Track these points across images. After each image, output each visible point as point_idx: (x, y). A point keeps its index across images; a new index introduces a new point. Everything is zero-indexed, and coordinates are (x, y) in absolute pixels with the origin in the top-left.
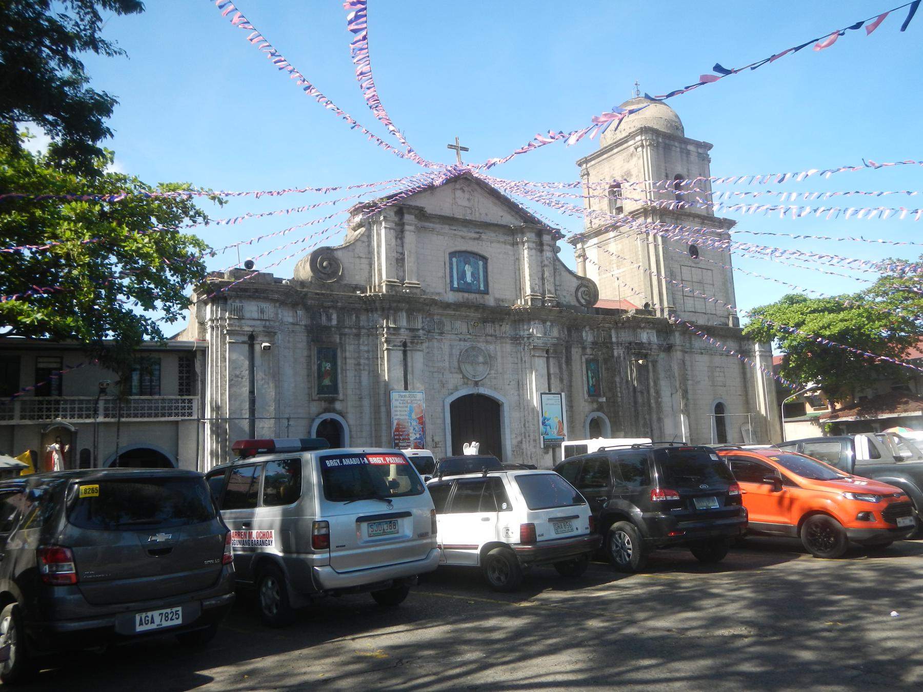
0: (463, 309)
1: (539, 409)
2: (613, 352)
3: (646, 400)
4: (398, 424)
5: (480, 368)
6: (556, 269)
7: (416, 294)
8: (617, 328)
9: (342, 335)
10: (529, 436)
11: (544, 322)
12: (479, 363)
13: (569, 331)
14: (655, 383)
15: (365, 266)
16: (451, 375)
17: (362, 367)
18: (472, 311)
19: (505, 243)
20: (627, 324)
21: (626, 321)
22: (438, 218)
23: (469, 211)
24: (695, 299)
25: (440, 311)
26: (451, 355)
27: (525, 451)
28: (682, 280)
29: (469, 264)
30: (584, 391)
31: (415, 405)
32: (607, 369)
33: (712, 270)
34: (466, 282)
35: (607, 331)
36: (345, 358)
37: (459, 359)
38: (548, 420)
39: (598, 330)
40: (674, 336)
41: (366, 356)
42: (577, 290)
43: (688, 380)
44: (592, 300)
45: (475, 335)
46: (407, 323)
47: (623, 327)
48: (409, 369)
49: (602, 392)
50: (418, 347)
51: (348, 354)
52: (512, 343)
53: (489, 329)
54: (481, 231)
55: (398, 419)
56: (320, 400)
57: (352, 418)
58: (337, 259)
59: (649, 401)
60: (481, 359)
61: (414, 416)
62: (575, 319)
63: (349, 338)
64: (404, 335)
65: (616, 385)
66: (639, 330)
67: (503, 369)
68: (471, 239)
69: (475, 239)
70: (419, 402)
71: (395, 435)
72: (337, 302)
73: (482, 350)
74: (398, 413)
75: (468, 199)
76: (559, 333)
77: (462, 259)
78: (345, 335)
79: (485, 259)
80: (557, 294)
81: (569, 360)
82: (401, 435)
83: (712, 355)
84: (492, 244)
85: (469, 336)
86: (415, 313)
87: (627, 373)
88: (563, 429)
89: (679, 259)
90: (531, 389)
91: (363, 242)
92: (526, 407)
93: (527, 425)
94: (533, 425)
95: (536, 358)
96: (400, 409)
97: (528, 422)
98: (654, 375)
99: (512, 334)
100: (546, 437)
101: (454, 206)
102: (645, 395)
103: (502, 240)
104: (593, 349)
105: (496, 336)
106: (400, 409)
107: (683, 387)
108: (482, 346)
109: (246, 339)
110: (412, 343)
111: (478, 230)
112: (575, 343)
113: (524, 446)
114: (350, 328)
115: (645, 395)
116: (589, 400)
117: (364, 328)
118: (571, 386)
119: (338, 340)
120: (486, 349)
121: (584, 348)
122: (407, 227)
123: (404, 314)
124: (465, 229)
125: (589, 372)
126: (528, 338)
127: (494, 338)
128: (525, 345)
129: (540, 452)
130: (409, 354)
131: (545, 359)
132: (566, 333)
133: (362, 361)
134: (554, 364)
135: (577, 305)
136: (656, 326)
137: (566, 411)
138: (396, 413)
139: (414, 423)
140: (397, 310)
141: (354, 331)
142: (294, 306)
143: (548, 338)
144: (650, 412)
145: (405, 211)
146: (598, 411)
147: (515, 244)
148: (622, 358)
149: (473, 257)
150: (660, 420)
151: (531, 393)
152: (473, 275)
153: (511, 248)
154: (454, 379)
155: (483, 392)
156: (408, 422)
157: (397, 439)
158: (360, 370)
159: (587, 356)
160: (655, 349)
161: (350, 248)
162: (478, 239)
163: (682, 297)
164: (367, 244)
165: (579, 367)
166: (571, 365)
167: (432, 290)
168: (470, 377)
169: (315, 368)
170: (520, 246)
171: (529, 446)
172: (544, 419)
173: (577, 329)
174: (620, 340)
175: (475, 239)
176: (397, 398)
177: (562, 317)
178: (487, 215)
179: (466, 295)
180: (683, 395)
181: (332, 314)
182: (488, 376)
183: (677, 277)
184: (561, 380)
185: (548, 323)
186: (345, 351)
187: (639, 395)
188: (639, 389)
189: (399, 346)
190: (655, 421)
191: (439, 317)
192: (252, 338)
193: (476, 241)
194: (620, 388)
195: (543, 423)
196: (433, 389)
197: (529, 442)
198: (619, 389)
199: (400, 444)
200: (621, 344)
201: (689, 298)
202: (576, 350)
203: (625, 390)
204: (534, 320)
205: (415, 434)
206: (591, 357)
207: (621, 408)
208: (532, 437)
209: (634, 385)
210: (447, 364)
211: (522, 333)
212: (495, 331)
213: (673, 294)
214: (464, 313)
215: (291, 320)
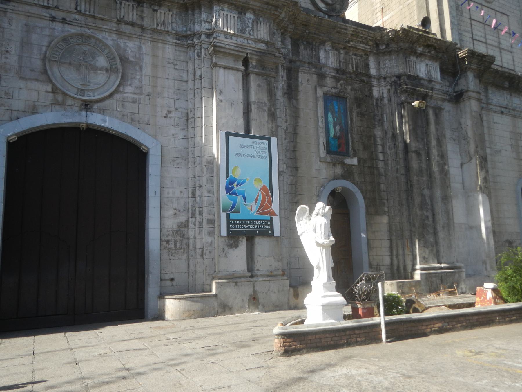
1: (222, 161)
2: (371, 90)
3: (424, 166)
5: (100, 78)
8: (378, 54)
10: (201, 213)
12: (95, 69)
13: (295, 44)
16: (22, 84)
20: (393, 46)
21: (392, 40)
24: (488, 46)
27: (191, 241)
28: (471, 19)
30: (318, 145)
32: (361, 115)
33: (508, 16)
35: (361, 56)
37: (46, 52)
39: (346, 53)
40: (466, 77)
44: (338, 6)
45: (94, 17)
47: (388, 52)
49: (351, 149)
52: (177, 45)
60: (102, 61)
62: (306, 25)
66: (413, 58)
67: (154, 87)
73: (106, 46)
76: (272, 35)
85: (77, 16)
87: (393, 122)
88: (270, 203)
90: (209, 126)
92: (198, 160)
93: (198, 193)
94: (209, 192)
95: (221, 71)
97: (201, 186)
98: (437, 130)
99: (180, 30)
100: (233, 215)
102: (424, 157)
104: (337, 79)
105: (142, 27)
107: (481, 152)
112: (306, 65)
113: (191, 233)
115: (424, 157)
116: (329, 159)
118: (295, 133)
120: (118, 47)
125: (330, 115)
126: (209, 35)
127: (138, 31)
128: (201, 49)
129: (219, 243)
131: (240, 75)
132: (290, 47)
134: (259, 86)
135: (311, 7)
136: (440, 55)
137: (280, 173)
143: (248, 39)
144: (430, 187)
146: (345, 179)
148: (386, 101)
150: (446, 198)
151: (209, 134)
155: (101, 124)
159: (326, 89)
160: (438, 90)
163: (471, 40)
165: (311, 105)
166: (297, 100)
168: (72, 93)
171: (200, 231)
172: (232, 182)
173: (308, 43)
174: (383, 73)
180: (481, 164)
182: (117, 96)
183: (464, 14)
184: (272, 116)
185: (250, 16)
187: (413, 156)
188: (413, 146)
190: (440, 199)
194: (383, 146)
195: (229, 189)
197: (201, 224)
198: (380, 148)
200: (385, 78)
201: (480, 43)
202: (307, 76)
203: (390, 149)
206: (334, 91)
207: (383, 178)
208: (205, 215)
209: (405, 142)
211: (197, 28)
212: (142, 18)
213: (460, 34)
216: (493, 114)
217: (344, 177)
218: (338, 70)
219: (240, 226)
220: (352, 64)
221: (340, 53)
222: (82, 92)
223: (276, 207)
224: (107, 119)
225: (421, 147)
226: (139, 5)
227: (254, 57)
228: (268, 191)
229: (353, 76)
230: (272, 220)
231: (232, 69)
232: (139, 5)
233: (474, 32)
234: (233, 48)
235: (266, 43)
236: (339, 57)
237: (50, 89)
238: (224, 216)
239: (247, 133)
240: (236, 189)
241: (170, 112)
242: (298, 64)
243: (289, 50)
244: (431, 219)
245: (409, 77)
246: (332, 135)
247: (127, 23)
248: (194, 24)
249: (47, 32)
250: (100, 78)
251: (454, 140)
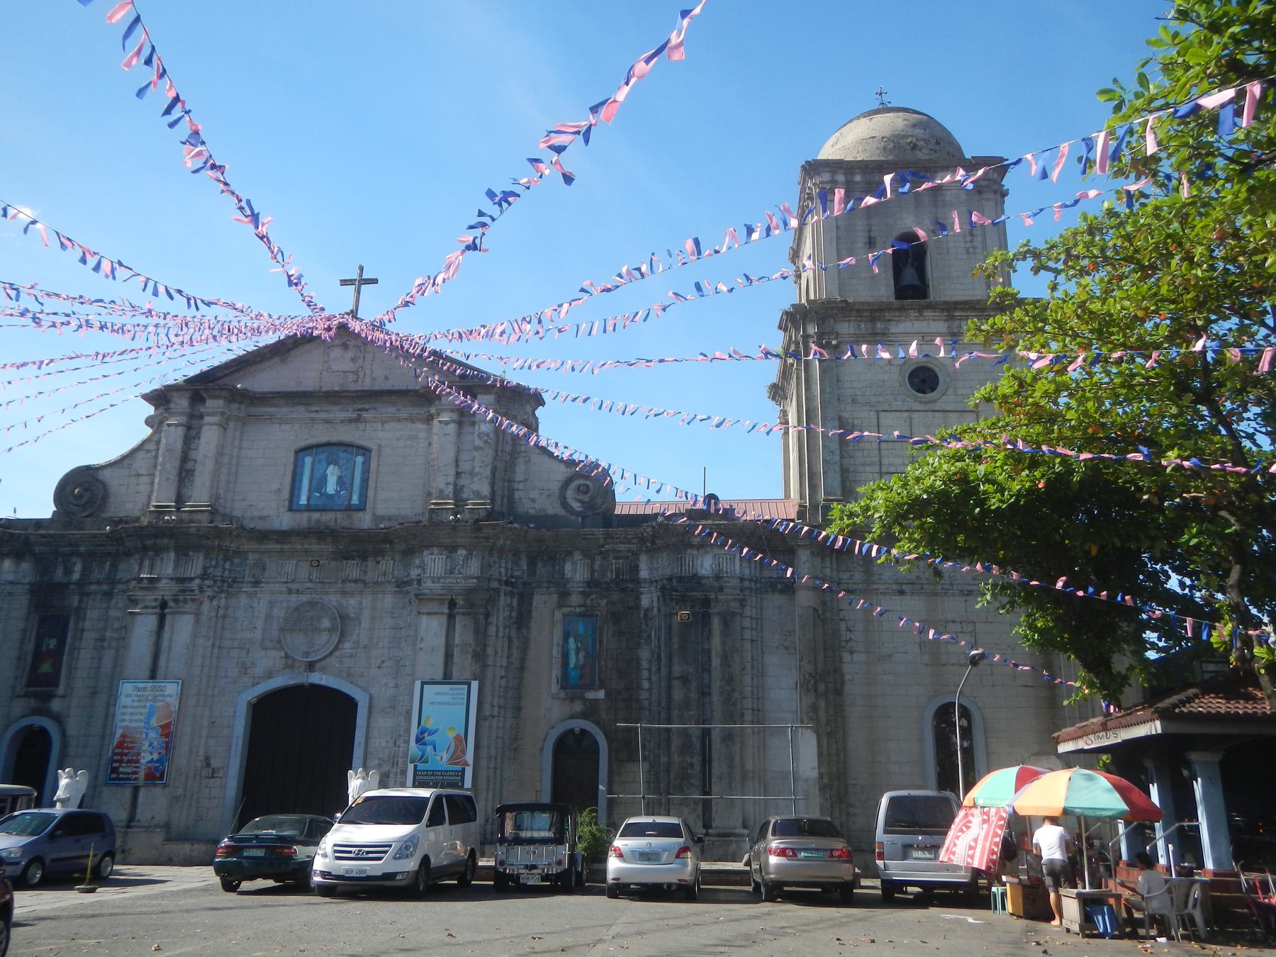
0: (294, 539)
2: (638, 599)
4: (123, 736)
6: (520, 452)
7: (200, 521)
8: (648, 551)
9: (84, 595)
11: (452, 549)
13: (532, 563)
14: (726, 660)
15: (144, 488)
16: (263, 654)
17: (106, 644)
18: (314, 541)
19: (411, 419)
20: (658, 541)
21: (653, 535)
22: (282, 397)
23: (351, 377)
25: (254, 546)
26: (269, 618)
29: (336, 463)
31: (160, 704)
36: (82, 630)
38: (432, 733)
41: (117, 625)
42: (566, 484)
43: (852, 653)
46: (174, 569)
48: (165, 644)
50: (190, 607)
51: (87, 625)
52: (396, 592)
53: (353, 569)
55: (126, 727)
56: (26, 695)
57: (73, 727)
58: (103, 484)
59: (705, 693)
60: (326, 623)
61: (154, 723)
63: (94, 599)
64: (166, 589)
65: (638, 663)
68: (342, 421)
69: (350, 421)
70: (168, 699)
71: (115, 754)
72: (79, 546)
74: (127, 717)
75: (353, 360)
76: (485, 566)
77: (323, 456)
78: (89, 594)
79: (365, 451)
81: (522, 619)
82: (126, 755)
83: (936, 594)
84: (387, 426)
85: (309, 585)
86: (191, 553)
88: (464, 752)
89: (874, 399)
91: (149, 451)
95: (424, 619)
96: (131, 710)
98: (724, 643)
100: (421, 766)
101: (325, 373)
103: (404, 416)
104: (585, 594)
105: (364, 582)
106: (131, 710)
108: (333, 600)
110: (176, 601)
111: (360, 407)
114: (99, 583)
116: (562, 695)
117: (120, 582)
119: (75, 603)
121: (564, 594)
122: (207, 419)
123: (172, 555)
124: (335, 408)
127: (361, 585)
130: (169, 619)
131: (445, 618)
132: (525, 568)
133: (108, 634)
134: (465, 626)
135: (561, 512)
138: (123, 717)
139: (153, 735)
140: (159, 551)
142: (18, 556)
145: (204, 395)
147: (429, 419)
149: (345, 451)
152: (340, 480)
153: (424, 426)
154: (266, 659)
156: (141, 733)
157: (116, 761)
158: (103, 648)
160: (734, 588)
161: (126, 462)
162: (358, 420)
164: (153, 454)
166: (528, 628)
167: (256, 514)
169: (30, 647)
170: (435, 422)
172: (422, 733)
175: (350, 421)
176: (130, 691)
177: (487, 538)
178: (386, 378)
179: (316, 515)
181: (75, 564)
182: (337, 653)
184: (480, 656)
185: (462, 552)
186: (85, 619)
187: (676, 684)
189: (154, 607)
191: (257, 556)
193: (353, 425)
195: (419, 740)
196: (226, 677)
198: (645, 674)
199: (121, 769)
204: (427, 547)
205: (151, 753)
206: (578, 610)
210: (258, 634)
212: (366, 572)
214: (299, 547)
215: (11, 577)
216: (880, 597)
217: (584, 715)
218: (589, 583)
219: (426, 778)
220: (612, 571)
221: (593, 561)
222: (307, 654)
223: (469, 757)
224: (324, 676)
225: (691, 670)
226: (363, 561)
227: (458, 597)
228: (461, 741)
229: (613, 585)
230: (464, 769)
231: (436, 613)
232: (363, 561)
233: (885, 461)
234: (440, 592)
235: (477, 578)
236: (592, 564)
237: (283, 655)
238: (411, 767)
239: (447, 679)
240: (427, 738)
241: (383, 662)
242: (535, 585)
243: (523, 572)
244: (697, 768)
245: (680, 579)
246: (572, 664)
247: (351, 581)
249: (285, 604)
250: (324, 638)
251: (787, 648)
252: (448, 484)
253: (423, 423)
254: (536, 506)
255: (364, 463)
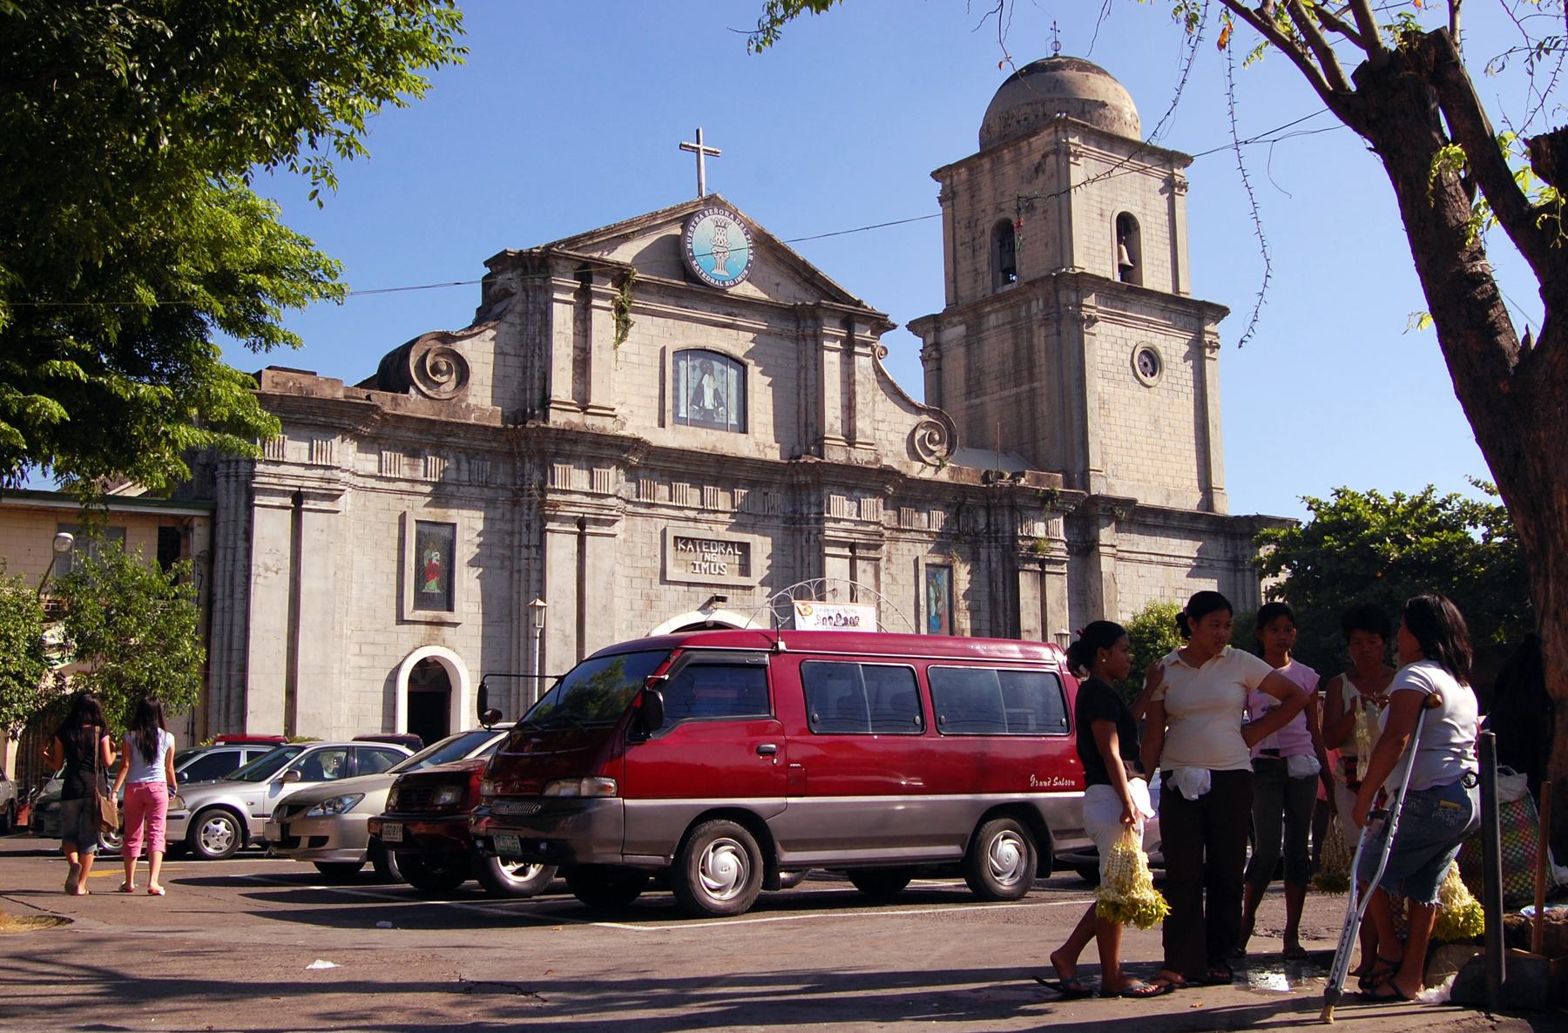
29: (711, 374)
34: (702, 408)
54: (736, 311)
77: (697, 362)
80: (877, 437)
91: (512, 325)
109: (288, 501)
111: (730, 311)
125: (931, 588)
128: (809, 534)
131: (847, 561)
141: (487, 493)
152: (716, 394)
153: (792, 345)
192: (298, 497)
246: (933, 614)
248: (802, 505)
251: (1080, 605)
252: (837, 418)
253: (792, 342)
254: (893, 449)
255: (738, 376)
